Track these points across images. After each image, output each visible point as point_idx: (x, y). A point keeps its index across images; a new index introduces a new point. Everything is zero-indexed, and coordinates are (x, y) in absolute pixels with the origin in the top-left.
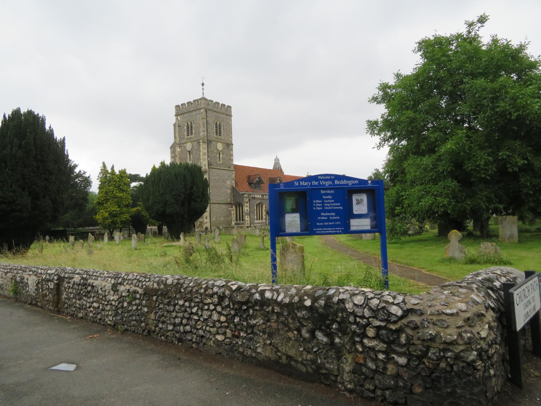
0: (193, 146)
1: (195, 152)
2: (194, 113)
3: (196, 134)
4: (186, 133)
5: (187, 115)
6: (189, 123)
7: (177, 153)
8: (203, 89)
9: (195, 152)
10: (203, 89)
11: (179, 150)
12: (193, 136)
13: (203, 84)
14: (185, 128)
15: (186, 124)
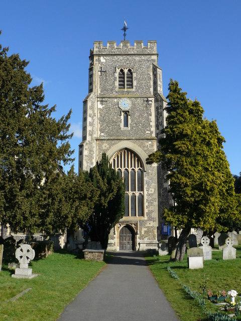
0: (133, 104)
1: (137, 114)
2: (137, 58)
3: (138, 88)
4: (117, 83)
5: (121, 58)
6: (126, 71)
7: (96, 112)
8: (125, 35)
9: (137, 114)
10: (125, 35)
11: (100, 106)
12: (134, 90)
13: (125, 29)
14: (117, 75)
15: (118, 71)
